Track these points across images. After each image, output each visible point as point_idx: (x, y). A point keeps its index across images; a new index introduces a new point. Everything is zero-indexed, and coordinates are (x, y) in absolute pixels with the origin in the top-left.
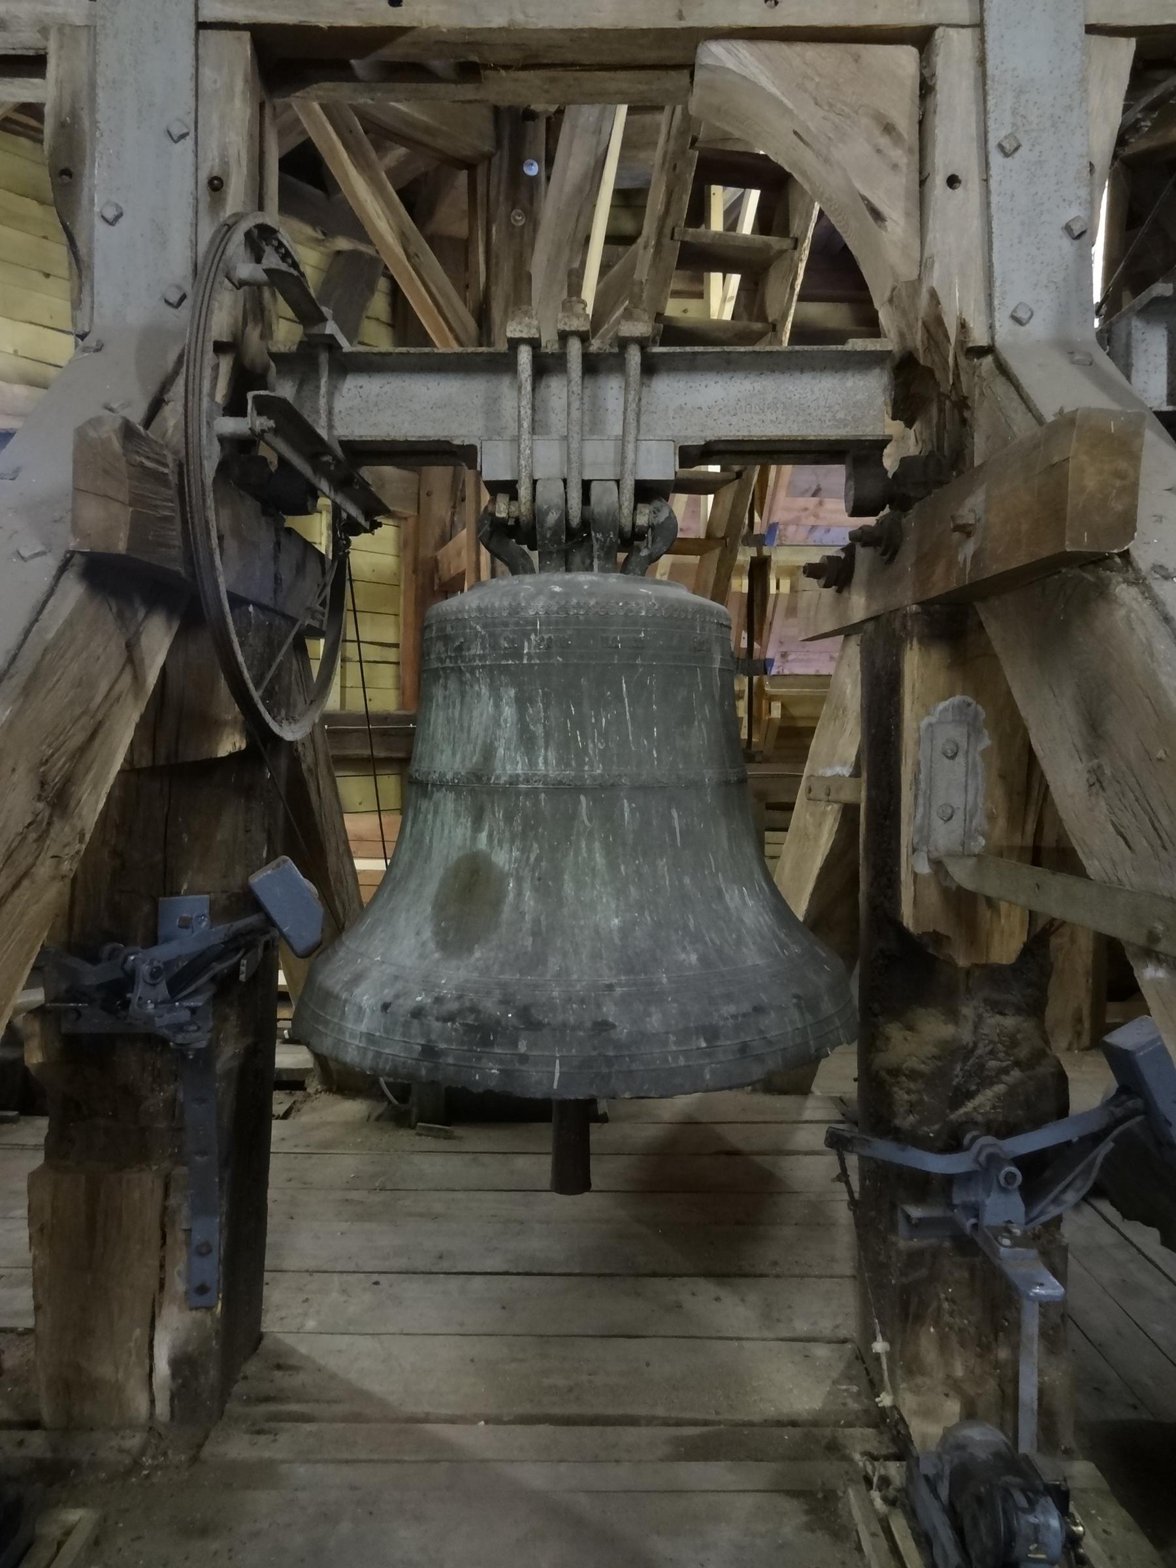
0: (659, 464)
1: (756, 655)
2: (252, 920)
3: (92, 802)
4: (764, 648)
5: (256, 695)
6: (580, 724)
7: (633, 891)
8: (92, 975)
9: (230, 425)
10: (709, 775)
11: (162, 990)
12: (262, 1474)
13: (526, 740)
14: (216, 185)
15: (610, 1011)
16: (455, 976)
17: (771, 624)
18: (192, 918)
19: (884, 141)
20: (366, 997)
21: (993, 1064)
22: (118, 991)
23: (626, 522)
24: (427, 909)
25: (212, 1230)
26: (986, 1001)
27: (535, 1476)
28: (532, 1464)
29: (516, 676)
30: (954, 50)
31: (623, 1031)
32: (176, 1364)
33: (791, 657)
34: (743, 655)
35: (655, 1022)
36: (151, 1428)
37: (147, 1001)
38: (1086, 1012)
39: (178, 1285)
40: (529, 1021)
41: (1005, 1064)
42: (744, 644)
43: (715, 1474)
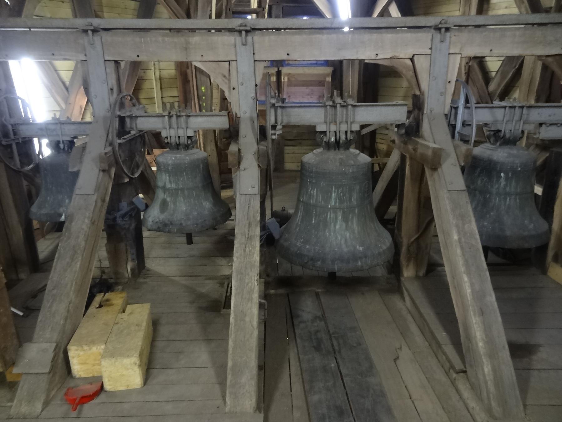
0: (190, 133)
2: (133, 206)
3: (108, 198)
4: (283, 95)
5: (129, 174)
6: (178, 179)
7: (187, 204)
8: (111, 217)
9: (119, 141)
10: (200, 185)
11: (121, 219)
12: (145, 283)
13: (170, 182)
14: (112, 89)
15: (183, 222)
16: (162, 217)
18: (124, 206)
19: (224, 79)
20: (150, 220)
22: (115, 219)
23: (186, 143)
24: (158, 206)
25: (134, 251)
27: (184, 282)
28: (184, 281)
29: (169, 172)
30: (233, 64)
31: (184, 225)
32: (131, 270)
35: (189, 223)
36: (129, 278)
37: (119, 221)
39: (130, 259)
40: (171, 223)
43: (210, 281)
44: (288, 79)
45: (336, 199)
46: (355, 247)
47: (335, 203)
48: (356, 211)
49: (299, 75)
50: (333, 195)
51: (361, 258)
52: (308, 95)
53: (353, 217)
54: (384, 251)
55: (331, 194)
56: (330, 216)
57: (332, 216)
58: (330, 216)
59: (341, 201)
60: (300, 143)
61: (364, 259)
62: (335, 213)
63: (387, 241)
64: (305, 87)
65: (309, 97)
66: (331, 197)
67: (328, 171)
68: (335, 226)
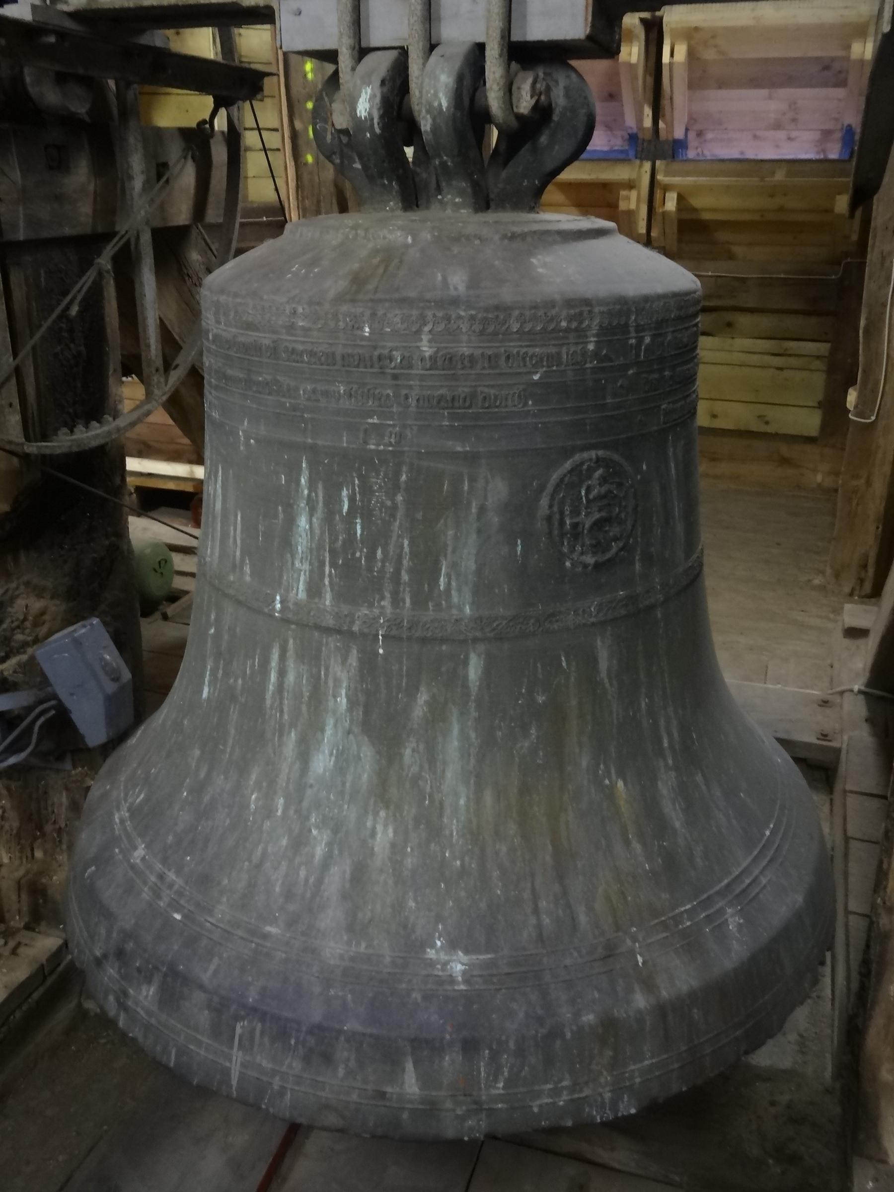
1: (663, 135)
4: (670, 126)
17: (671, 99)
21: (19, 637)
26: (27, 584)
33: (709, 136)
34: (648, 136)
38: (872, 561)
41: (29, 639)
42: (648, 122)
44: (691, 54)
45: (315, 551)
46: (414, 946)
47: (314, 590)
48: (474, 670)
49: (733, 32)
50: (303, 522)
51: (426, 1047)
52: (777, 126)
53: (437, 715)
54: (661, 1010)
55: (291, 521)
56: (282, 673)
57: (291, 678)
58: (282, 673)
59: (355, 581)
60: (729, 325)
61: (450, 1062)
62: (311, 656)
63: (733, 922)
64: (764, 92)
65: (781, 135)
66: (287, 543)
67: (266, 340)
68: (304, 756)
